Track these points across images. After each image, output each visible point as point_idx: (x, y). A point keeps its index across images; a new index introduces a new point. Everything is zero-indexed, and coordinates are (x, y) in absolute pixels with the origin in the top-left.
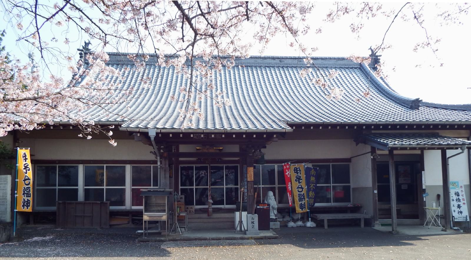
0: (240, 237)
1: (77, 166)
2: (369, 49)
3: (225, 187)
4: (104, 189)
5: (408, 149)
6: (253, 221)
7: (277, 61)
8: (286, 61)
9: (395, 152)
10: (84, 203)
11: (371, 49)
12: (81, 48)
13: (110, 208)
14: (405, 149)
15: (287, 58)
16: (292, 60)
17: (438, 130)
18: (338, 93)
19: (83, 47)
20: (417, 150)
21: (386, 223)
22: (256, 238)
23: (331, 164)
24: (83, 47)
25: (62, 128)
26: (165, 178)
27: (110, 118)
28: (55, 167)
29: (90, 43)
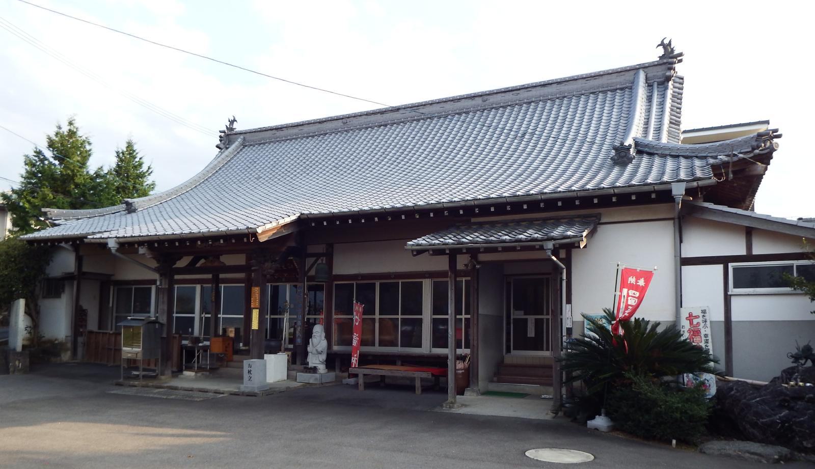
0: (216, 390)
1: (151, 288)
2: (659, 45)
3: (377, 316)
4: (374, 314)
5: (464, 251)
6: (250, 369)
7: (479, 101)
8: (492, 99)
9: (483, 257)
10: (96, 332)
11: (662, 44)
12: (225, 129)
13: (292, 345)
14: (494, 250)
15: (355, 116)
16: (503, 94)
17: (594, 208)
18: (56, 212)
19: (227, 126)
20: (500, 251)
21: (521, 392)
22: (232, 393)
23: (400, 281)
24: (227, 126)
25: (418, 217)
26: (163, 302)
27: (558, 187)
28: (132, 288)
29: (236, 121)
